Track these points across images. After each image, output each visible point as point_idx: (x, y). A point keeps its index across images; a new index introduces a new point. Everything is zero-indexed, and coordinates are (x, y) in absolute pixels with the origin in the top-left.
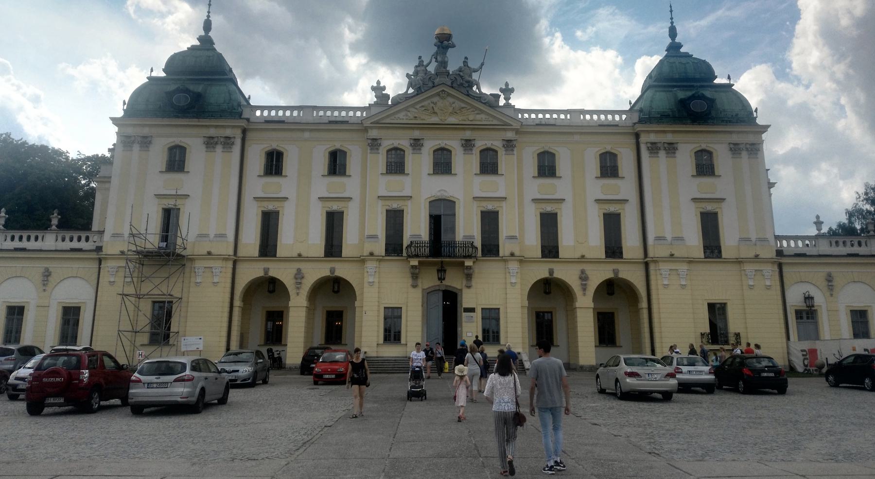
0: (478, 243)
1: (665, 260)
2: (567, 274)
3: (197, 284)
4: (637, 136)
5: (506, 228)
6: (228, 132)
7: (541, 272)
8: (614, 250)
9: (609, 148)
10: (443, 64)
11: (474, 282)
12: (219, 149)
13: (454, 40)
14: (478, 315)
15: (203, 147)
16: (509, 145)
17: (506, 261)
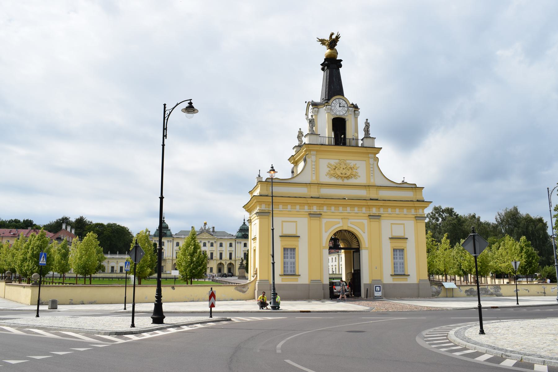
0: (210, 258)
1: (238, 260)
2: (223, 262)
3: (167, 263)
4: (236, 240)
5: (214, 255)
6: (171, 240)
7: (219, 262)
8: (230, 258)
9: (231, 242)
10: (205, 228)
11: (209, 263)
12: (169, 242)
13: (207, 224)
14: (209, 268)
15: (167, 242)
16: (215, 242)
17: (214, 260)
